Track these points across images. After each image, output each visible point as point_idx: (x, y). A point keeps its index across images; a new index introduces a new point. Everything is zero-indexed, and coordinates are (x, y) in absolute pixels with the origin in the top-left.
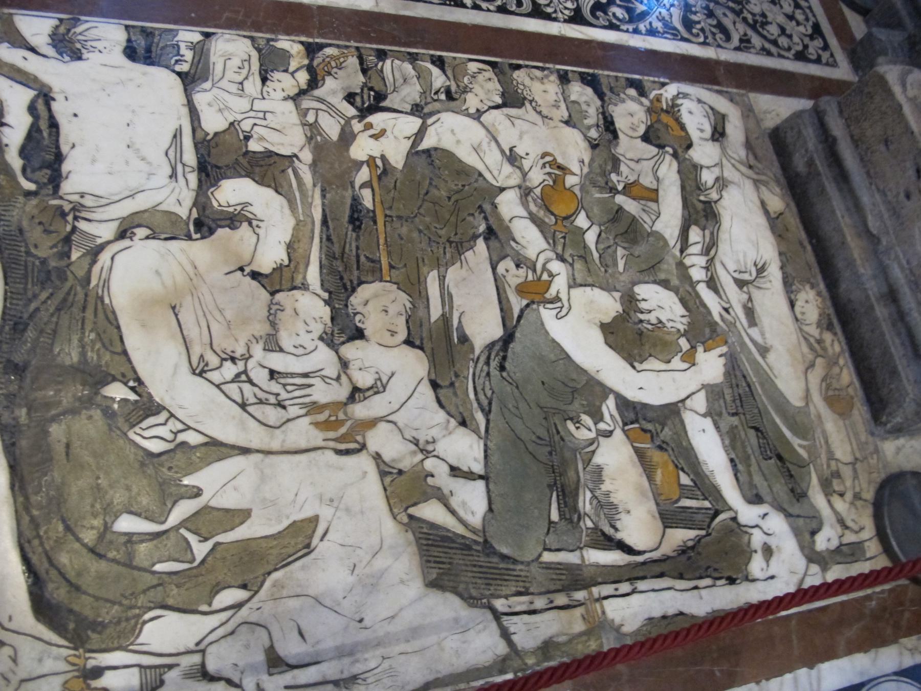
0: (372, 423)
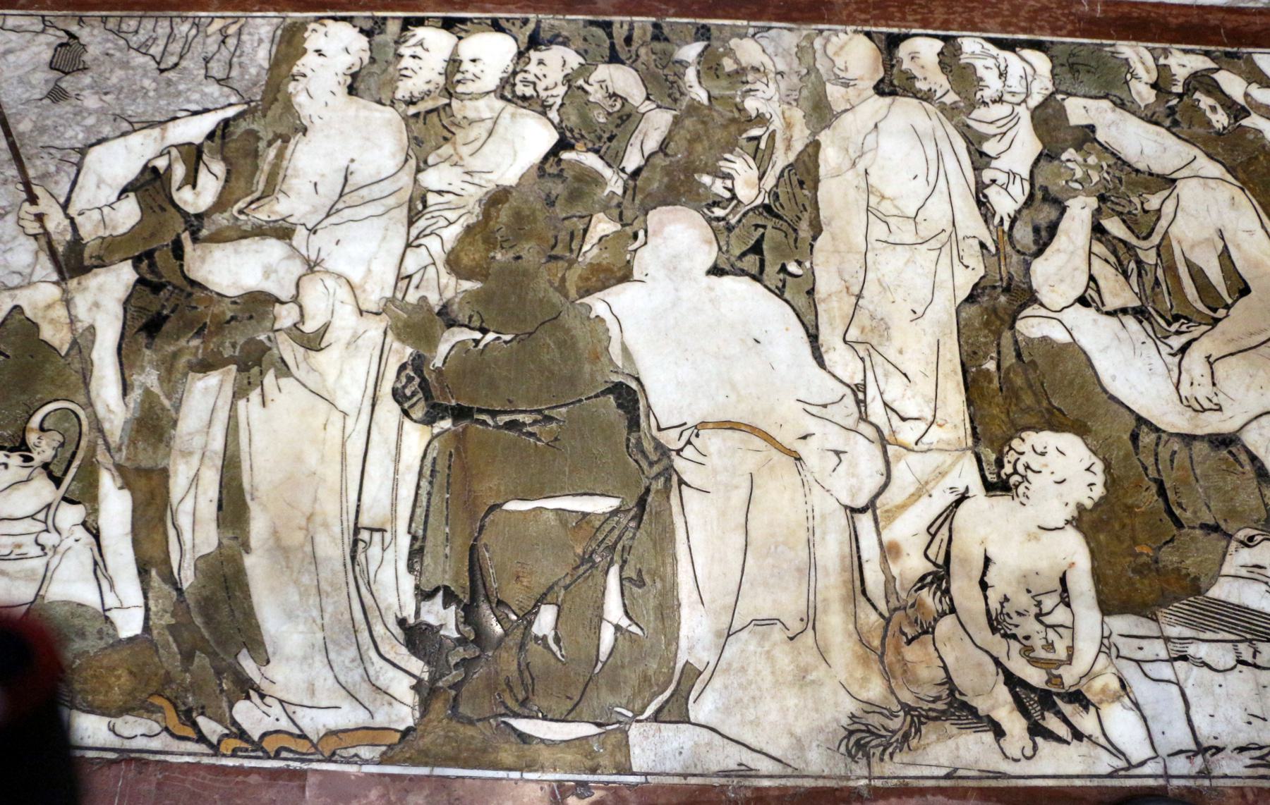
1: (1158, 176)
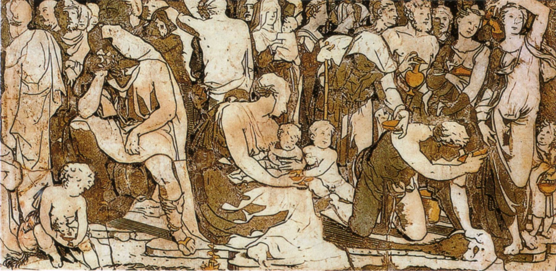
0: (312, 178)
1: (133, 60)
